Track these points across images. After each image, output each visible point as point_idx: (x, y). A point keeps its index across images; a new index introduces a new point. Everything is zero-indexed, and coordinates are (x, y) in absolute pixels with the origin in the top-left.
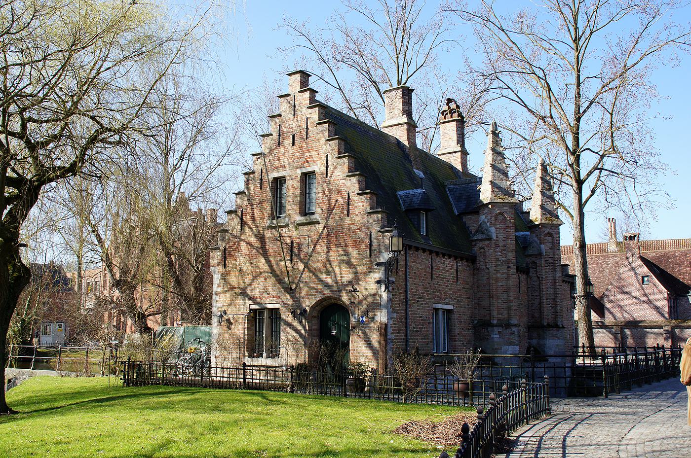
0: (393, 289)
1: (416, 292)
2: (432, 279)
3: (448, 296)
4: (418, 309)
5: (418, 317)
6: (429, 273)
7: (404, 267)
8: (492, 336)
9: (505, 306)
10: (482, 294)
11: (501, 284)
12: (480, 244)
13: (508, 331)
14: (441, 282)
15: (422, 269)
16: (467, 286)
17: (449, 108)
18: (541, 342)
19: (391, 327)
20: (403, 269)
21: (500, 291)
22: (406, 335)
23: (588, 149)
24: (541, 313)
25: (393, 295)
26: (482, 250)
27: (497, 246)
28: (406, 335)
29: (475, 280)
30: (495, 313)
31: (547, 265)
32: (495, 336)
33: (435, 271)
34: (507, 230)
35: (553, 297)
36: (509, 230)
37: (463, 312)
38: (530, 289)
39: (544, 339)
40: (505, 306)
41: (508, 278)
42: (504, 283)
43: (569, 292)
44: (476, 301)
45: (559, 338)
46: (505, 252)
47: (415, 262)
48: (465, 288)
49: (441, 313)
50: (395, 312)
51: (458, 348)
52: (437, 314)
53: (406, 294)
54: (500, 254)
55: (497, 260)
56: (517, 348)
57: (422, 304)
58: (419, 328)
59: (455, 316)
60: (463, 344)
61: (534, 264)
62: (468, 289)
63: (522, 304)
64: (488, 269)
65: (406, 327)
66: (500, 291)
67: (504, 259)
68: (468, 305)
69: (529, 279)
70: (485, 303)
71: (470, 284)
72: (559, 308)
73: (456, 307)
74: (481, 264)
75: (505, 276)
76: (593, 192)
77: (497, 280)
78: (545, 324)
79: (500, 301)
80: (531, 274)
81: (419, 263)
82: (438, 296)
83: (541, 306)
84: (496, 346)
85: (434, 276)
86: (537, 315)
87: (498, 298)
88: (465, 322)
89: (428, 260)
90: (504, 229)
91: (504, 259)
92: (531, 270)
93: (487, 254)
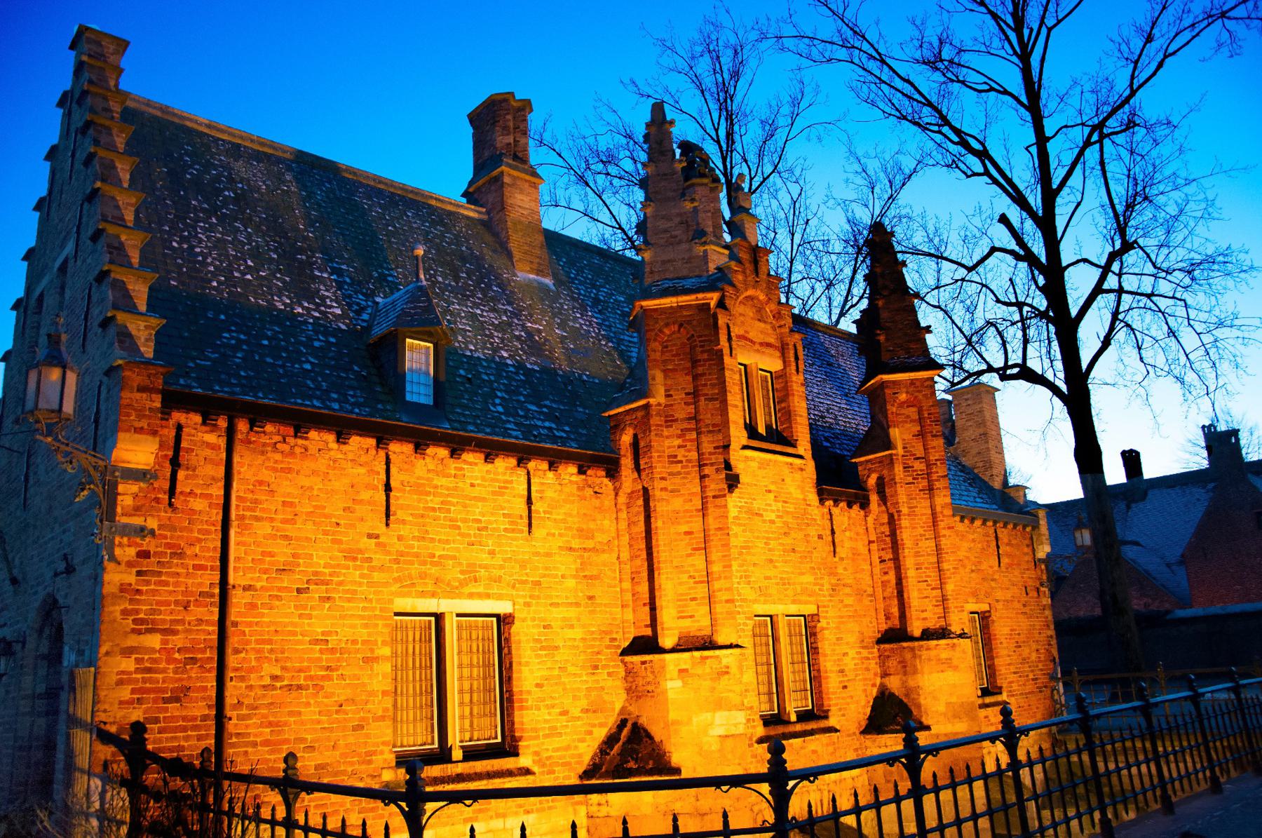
0: (144, 554)
5: (299, 642)
18: (911, 683)
19: (120, 683)
23: (1085, 261)
25: (139, 573)
39: (915, 672)
45: (955, 668)
51: (536, 730)
56: (740, 717)
58: (311, 678)
76: (1106, 343)
82: (423, 576)
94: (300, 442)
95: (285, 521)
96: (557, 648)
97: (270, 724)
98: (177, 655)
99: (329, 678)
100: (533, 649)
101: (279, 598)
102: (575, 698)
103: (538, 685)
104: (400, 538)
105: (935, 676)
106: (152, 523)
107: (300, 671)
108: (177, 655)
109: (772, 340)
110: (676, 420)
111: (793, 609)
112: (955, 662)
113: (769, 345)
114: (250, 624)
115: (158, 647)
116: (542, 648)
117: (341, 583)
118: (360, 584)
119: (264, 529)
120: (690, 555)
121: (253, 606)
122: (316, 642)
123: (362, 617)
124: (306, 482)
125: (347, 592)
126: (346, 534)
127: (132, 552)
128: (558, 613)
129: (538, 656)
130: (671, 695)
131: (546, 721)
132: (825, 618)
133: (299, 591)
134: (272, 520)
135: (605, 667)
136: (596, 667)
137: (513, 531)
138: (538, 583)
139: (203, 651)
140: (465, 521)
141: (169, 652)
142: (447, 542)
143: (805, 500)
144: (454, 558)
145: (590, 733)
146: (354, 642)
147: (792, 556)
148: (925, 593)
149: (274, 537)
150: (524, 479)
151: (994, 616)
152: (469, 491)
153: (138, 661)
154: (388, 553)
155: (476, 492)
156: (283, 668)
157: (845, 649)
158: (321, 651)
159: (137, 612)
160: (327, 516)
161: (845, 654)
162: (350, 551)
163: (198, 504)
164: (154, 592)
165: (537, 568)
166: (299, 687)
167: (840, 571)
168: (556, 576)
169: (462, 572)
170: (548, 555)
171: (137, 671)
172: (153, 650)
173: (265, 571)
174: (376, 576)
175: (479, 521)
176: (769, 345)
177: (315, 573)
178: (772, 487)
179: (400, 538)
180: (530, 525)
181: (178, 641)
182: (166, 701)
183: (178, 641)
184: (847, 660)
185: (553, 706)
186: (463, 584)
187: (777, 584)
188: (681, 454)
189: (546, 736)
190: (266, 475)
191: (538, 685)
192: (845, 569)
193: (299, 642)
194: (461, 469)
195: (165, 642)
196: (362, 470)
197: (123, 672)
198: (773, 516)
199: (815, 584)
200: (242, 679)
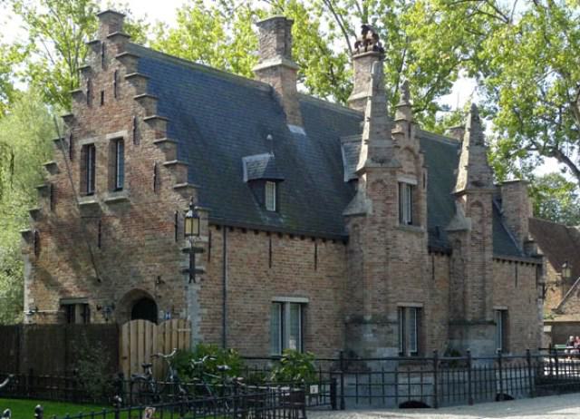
0: (202, 280)
2: (270, 266)
3: (299, 287)
4: (245, 303)
7: (222, 253)
8: (365, 335)
9: (382, 298)
11: (377, 270)
12: (354, 221)
13: (385, 329)
14: (288, 270)
17: (364, 37)
18: (464, 343)
19: (199, 325)
20: (221, 256)
22: (224, 335)
24: (465, 306)
25: (202, 287)
26: (356, 229)
28: (224, 335)
29: (348, 265)
30: (369, 307)
32: (368, 335)
33: (274, 256)
34: (388, 202)
35: (480, 285)
40: (382, 298)
41: (386, 264)
42: (382, 269)
43: (534, 277)
45: (487, 338)
46: (382, 230)
49: (288, 307)
50: (205, 307)
52: (283, 309)
53: (224, 285)
57: (252, 297)
59: (312, 312)
60: (325, 345)
63: (437, 294)
64: (362, 251)
65: (224, 325)
67: (383, 239)
69: (451, 263)
70: (358, 294)
72: (488, 299)
74: (353, 245)
75: (383, 260)
77: (372, 265)
78: (469, 320)
80: (454, 256)
84: (368, 348)
85: (274, 262)
86: (460, 308)
88: (328, 318)
89: (264, 243)
90: (384, 201)
91: (383, 239)
92: (455, 251)
93: (361, 233)
94: (243, 235)
96: (322, 318)
101: (238, 296)
104: (274, 272)
105: (476, 342)
111: (413, 305)
113: (411, 173)
121: (231, 299)
124: (246, 250)
128: (324, 303)
130: (368, 340)
150: (313, 246)
155: (298, 253)
163: (216, 261)
176: (411, 173)
178: (408, 247)
179: (274, 272)
186: (293, 290)
188: (378, 238)
198: (407, 260)
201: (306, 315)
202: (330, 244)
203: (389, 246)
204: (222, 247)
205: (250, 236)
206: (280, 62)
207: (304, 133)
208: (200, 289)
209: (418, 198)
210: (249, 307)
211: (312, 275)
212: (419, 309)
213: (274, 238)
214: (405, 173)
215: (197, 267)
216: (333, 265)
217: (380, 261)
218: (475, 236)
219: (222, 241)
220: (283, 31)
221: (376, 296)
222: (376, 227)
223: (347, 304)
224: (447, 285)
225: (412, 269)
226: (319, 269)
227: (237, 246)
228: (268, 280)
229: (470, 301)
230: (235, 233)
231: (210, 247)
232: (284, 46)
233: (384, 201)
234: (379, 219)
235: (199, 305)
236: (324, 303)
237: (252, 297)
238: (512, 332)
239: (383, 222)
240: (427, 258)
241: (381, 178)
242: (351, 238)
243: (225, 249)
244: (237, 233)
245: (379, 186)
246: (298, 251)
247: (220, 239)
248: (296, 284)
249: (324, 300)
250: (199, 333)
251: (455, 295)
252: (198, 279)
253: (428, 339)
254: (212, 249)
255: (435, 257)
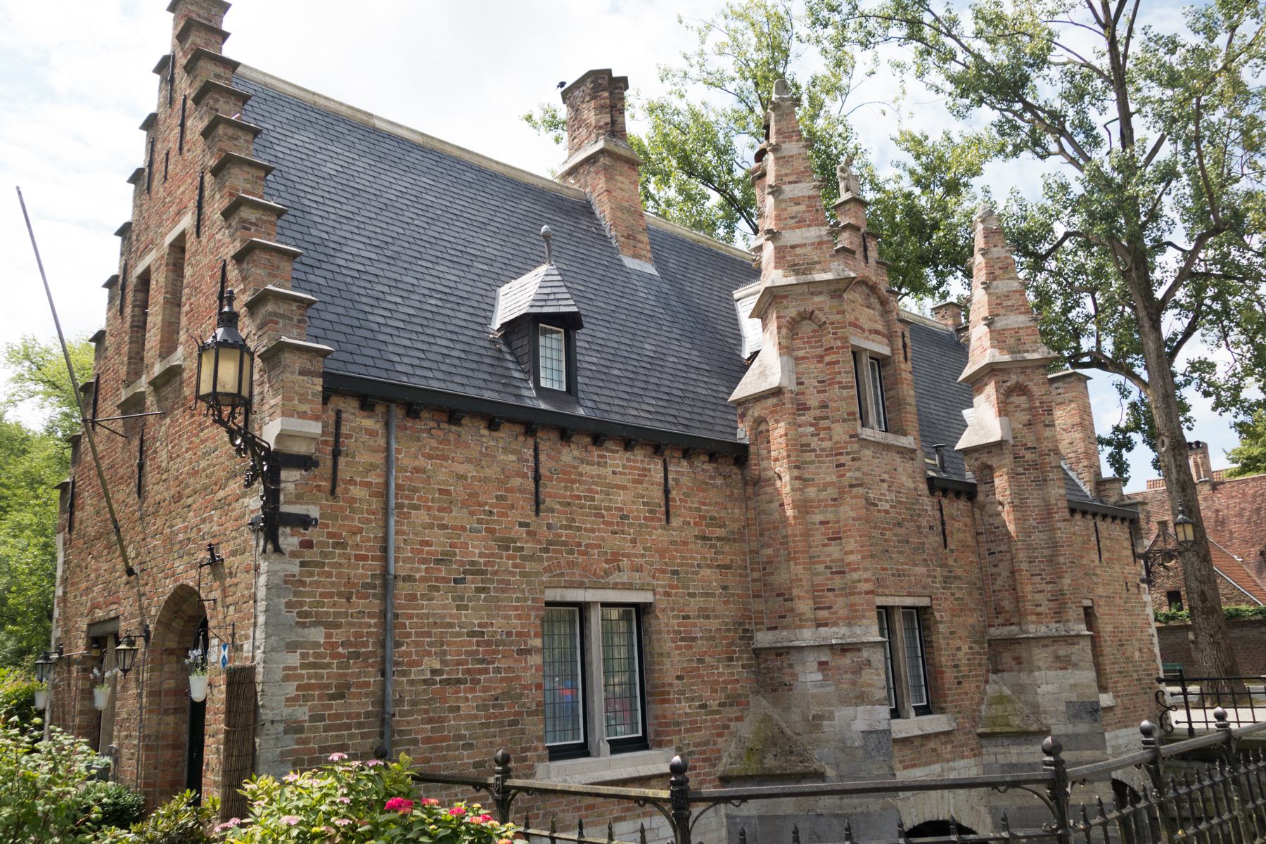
0: (307, 544)
1: (443, 553)
2: (537, 512)
3: (625, 562)
5: (459, 634)
6: (522, 491)
8: (802, 678)
9: (837, 582)
10: (769, 551)
11: (818, 518)
15: (486, 480)
16: (719, 532)
19: (286, 678)
20: (374, 478)
21: (818, 538)
22: (382, 702)
24: (1018, 600)
25: (303, 564)
27: (802, 408)
28: (382, 702)
31: (1021, 470)
34: (827, 359)
35: (1047, 552)
36: (833, 357)
37: (700, 609)
38: (982, 538)
42: (830, 516)
43: (1127, 544)
44: (756, 575)
45: (1075, 666)
47: (445, 458)
48: (705, 538)
51: (678, 724)
52: (584, 621)
53: (385, 559)
54: (811, 429)
55: (805, 447)
58: (468, 671)
61: (986, 472)
62: (718, 539)
65: (383, 675)
66: (818, 538)
67: (827, 444)
68: (725, 588)
71: (735, 526)
73: (667, 594)
75: (832, 492)
79: (820, 568)
81: (469, 461)
82: (571, 565)
83: (1014, 580)
84: (815, 710)
87: (812, 560)
90: (820, 358)
91: (827, 444)
94: (454, 428)
95: (440, 510)
96: (694, 639)
97: (431, 720)
98: (340, 650)
99: (486, 671)
100: (673, 641)
101: (437, 589)
102: (714, 691)
103: (678, 678)
104: (549, 526)
106: (314, 512)
107: (459, 663)
108: (340, 650)
109: (879, 327)
110: (809, 409)
111: (909, 601)
112: (1074, 658)
113: (877, 332)
114: (411, 617)
115: (322, 640)
116: (682, 639)
117: (495, 573)
118: (513, 574)
119: (421, 517)
120: (825, 545)
121: (412, 597)
122: (472, 634)
123: (516, 608)
124: (460, 469)
125: (499, 582)
126: (500, 523)
127: (295, 541)
128: (695, 603)
129: (678, 648)
131: (687, 714)
132: (939, 611)
133: (456, 581)
134: (429, 508)
135: (739, 659)
136: (731, 659)
137: (652, 519)
138: (675, 573)
139: (365, 644)
140: (608, 509)
141: (333, 646)
142: (592, 530)
143: (916, 489)
144: (599, 546)
145: (727, 727)
146: (509, 634)
147: (906, 548)
148: (1040, 587)
149: (431, 526)
150: (660, 467)
151: (1099, 612)
152: (611, 479)
153: (303, 656)
154: (539, 542)
155: (618, 480)
156: (443, 662)
157: (958, 643)
158: (478, 644)
159: (302, 604)
160: (481, 504)
161: (959, 649)
162: (502, 539)
163: (356, 492)
164: (317, 584)
165: (675, 558)
166: (459, 681)
167: (951, 562)
168: (692, 566)
169: (607, 562)
170: (685, 543)
171: (303, 666)
172: (316, 645)
173: (424, 561)
174: (528, 566)
175: (620, 509)
176: (877, 332)
177: (473, 563)
178: (886, 476)
179: (549, 526)
180: (667, 513)
181: (339, 635)
182: (332, 697)
183: (339, 635)
184: (960, 654)
185: (693, 699)
186: (607, 573)
187: (893, 575)
188: (814, 443)
189: (687, 731)
190: (421, 462)
191: (678, 678)
192: (955, 561)
193: (459, 634)
194: (603, 457)
195: (328, 636)
196: (513, 458)
197: (289, 668)
198: (887, 506)
199: (929, 576)
200: (404, 674)
201: (646, 631)
202: (704, 467)
203: (842, 459)
204: (379, 459)
205: (475, 437)
206: (601, 145)
207: (656, 273)
208: (294, 568)
209: (897, 381)
210: (471, 618)
211: (659, 535)
212: (922, 612)
213: (548, 442)
214: (863, 330)
215: (285, 508)
216: (713, 511)
217: (823, 495)
218: (1022, 452)
219: (381, 442)
220: (606, 94)
221: (818, 580)
222: (808, 417)
223: (756, 605)
224: (973, 558)
225: (900, 525)
226: (676, 522)
227: (430, 457)
228: (529, 546)
229: (1028, 588)
230: (426, 422)
231: (336, 454)
232: (608, 120)
233: (820, 358)
234: (813, 400)
235: (293, 616)
236: (695, 603)
237: (478, 590)
238: (1107, 650)
239: (824, 406)
240: (928, 503)
241: (809, 309)
242: (752, 449)
243: (388, 460)
244: (432, 424)
245: (807, 328)
246: (622, 477)
247: (372, 433)
248: (615, 558)
249: (692, 595)
250: (290, 701)
251: (994, 577)
252: (289, 540)
253: (949, 675)
254: (342, 461)
255: (945, 502)
